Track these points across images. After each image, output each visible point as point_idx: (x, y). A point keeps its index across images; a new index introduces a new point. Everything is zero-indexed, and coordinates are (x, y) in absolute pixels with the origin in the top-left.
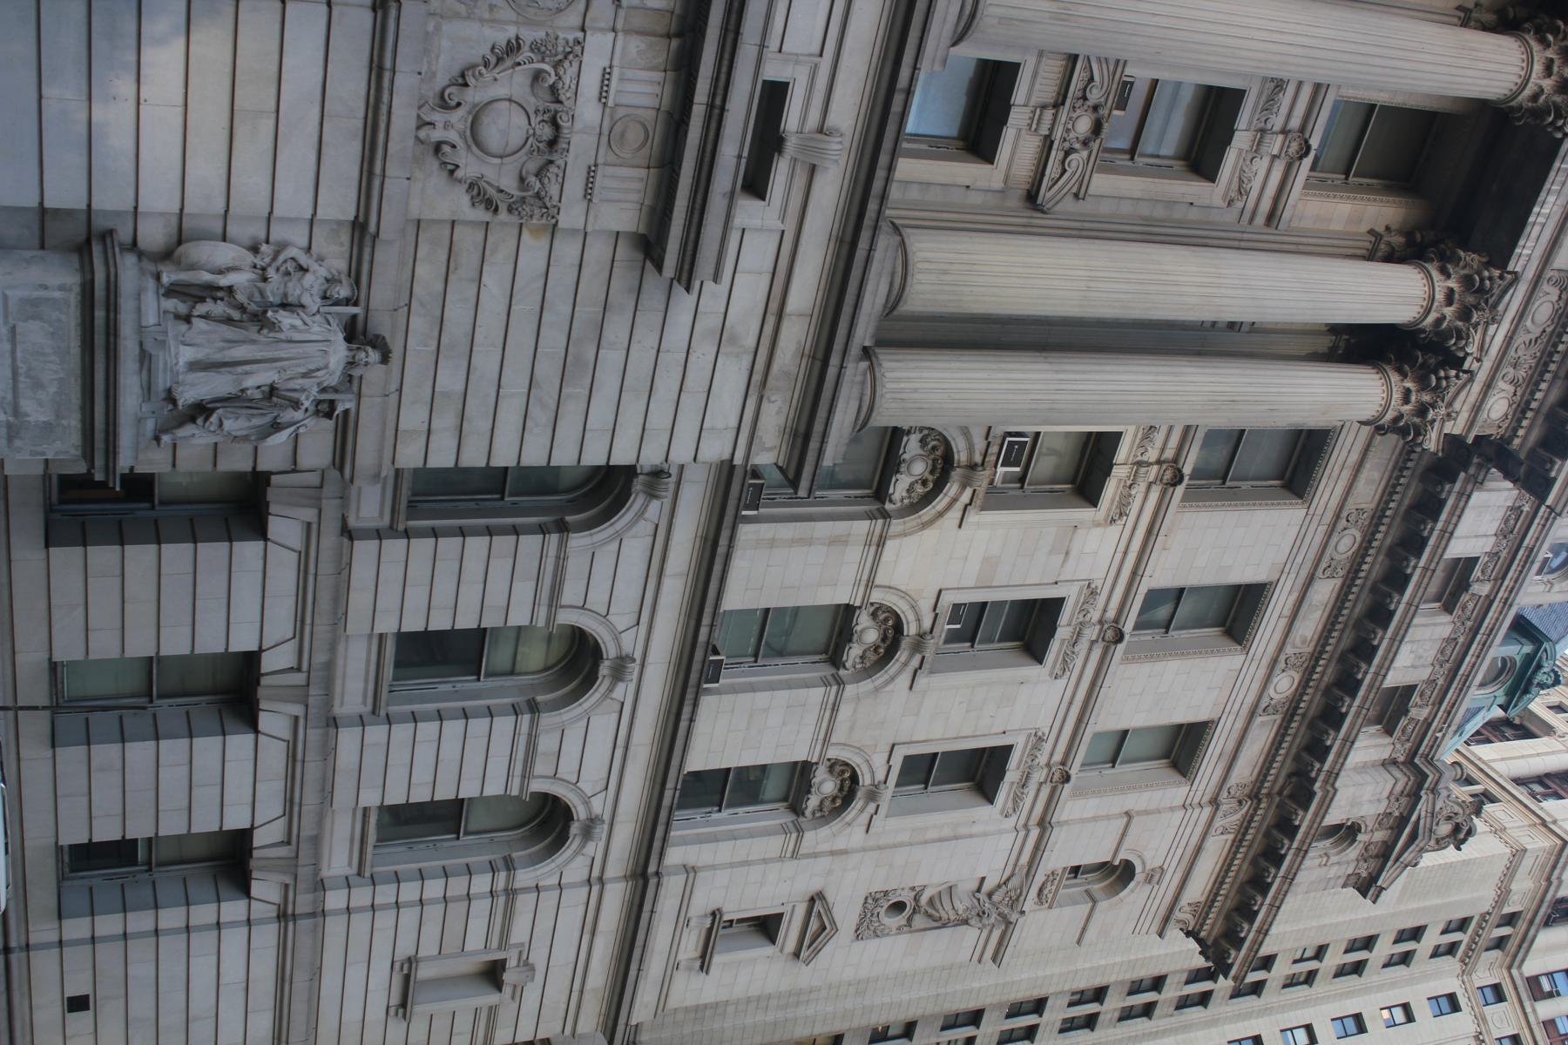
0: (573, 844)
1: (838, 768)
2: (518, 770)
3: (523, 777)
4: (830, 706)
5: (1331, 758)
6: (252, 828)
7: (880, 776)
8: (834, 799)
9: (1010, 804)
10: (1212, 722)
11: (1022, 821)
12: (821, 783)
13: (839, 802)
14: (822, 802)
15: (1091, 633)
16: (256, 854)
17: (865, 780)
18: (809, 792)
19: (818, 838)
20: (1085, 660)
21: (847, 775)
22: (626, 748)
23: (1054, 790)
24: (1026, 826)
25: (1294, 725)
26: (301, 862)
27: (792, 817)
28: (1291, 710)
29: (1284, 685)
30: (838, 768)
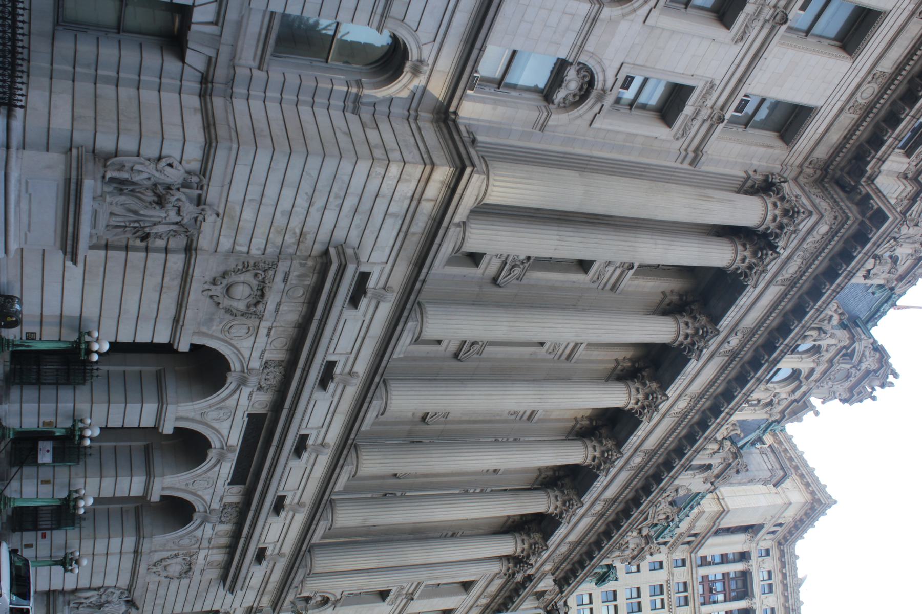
0: (405, 78)
1: (583, 73)
2: (379, 10)
3: (382, 16)
4: (590, 21)
5: (884, 148)
6: (194, 5)
7: (609, 84)
8: (574, 95)
9: (681, 132)
10: (816, 108)
11: (684, 147)
12: (569, 81)
13: (577, 98)
14: (567, 96)
15: (767, 13)
16: (193, 27)
17: (598, 85)
18: (560, 86)
19: (559, 119)
20: (756, 34)
21: (587, 79)
22: (454, 12)
23: (712, 126)
24: (686, 150)
25: (865, 124)
26: (223, 40)
27: (546, 104)
28: (869, 108)
29: (869, 91)
30: (583, 73)
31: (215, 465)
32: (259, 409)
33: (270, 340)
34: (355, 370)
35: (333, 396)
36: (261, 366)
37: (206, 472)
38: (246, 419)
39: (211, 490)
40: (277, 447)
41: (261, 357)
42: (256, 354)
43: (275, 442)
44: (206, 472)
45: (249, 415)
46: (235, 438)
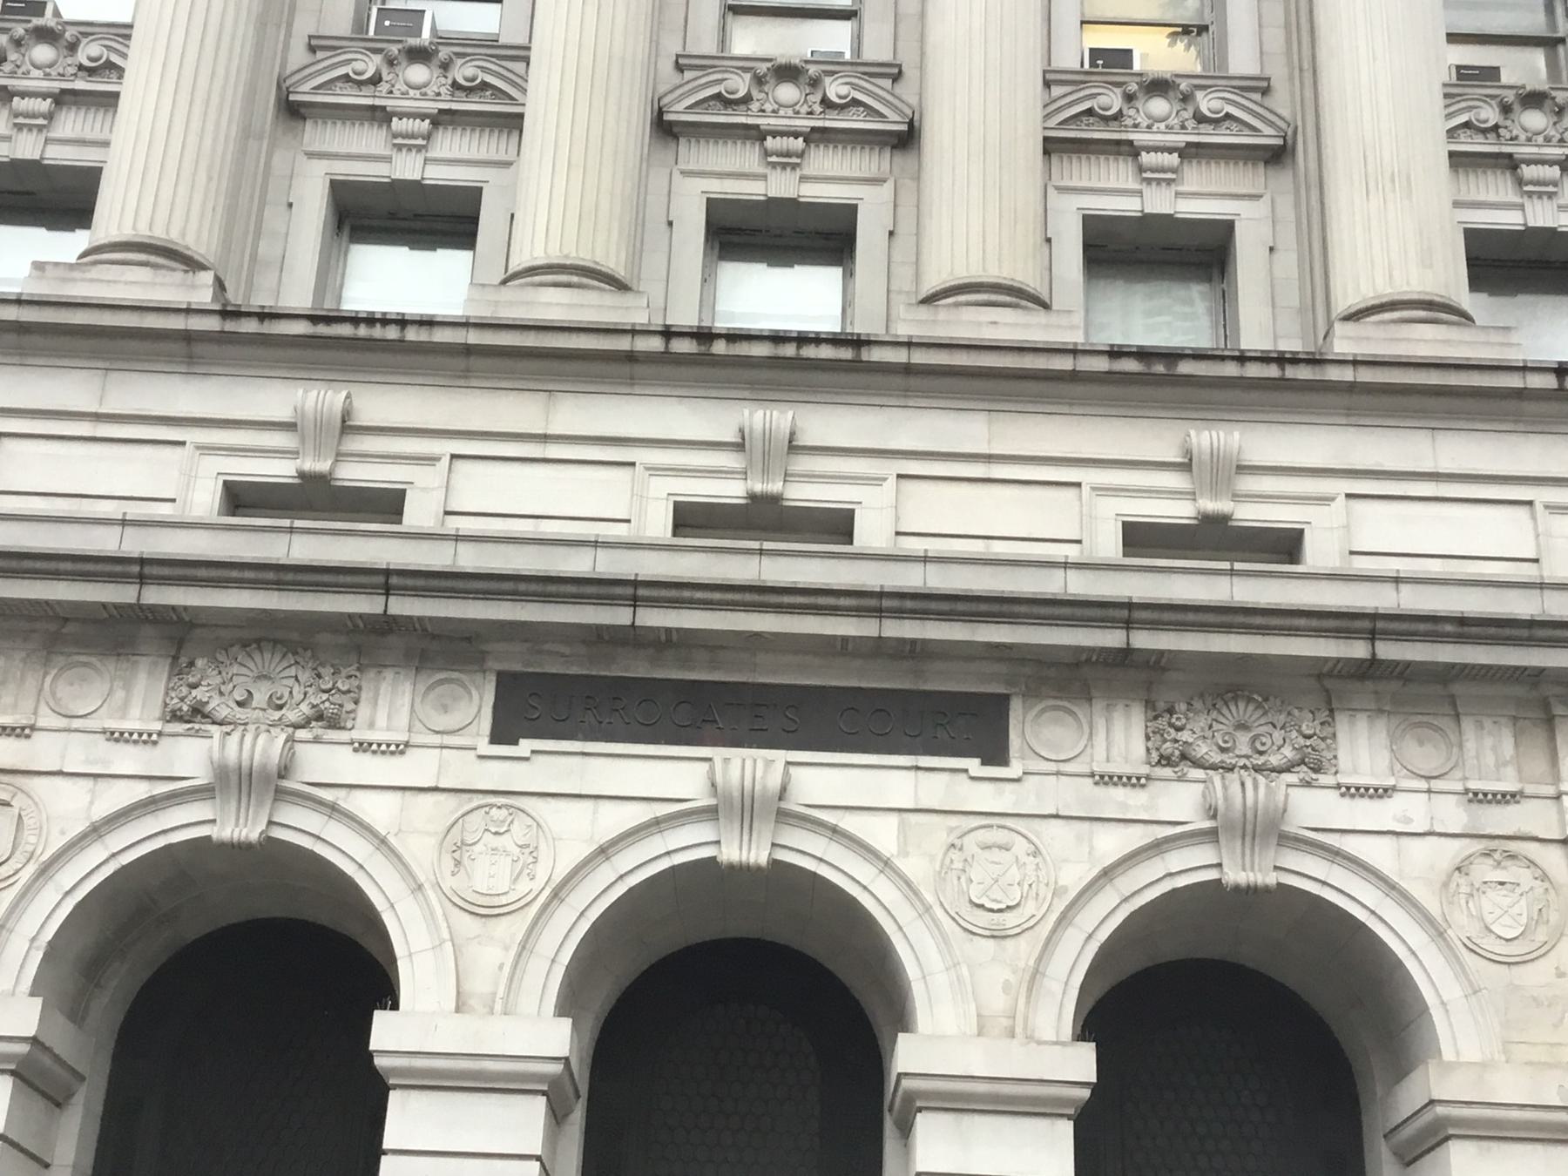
31: (835, 832)
32: (476, 705)
33: (46, 719)
34: (284, 415)
35: (432, 460)
36: (197, 734)
37: (885, 864)
38: (526, 746)
39: (1055, 836)
40: (635, 602)
41: (147, 740)
42: (128, 759)
43: (620, 616)
44: (885, 864)
45: (496, 739)
46: (675, 773)
